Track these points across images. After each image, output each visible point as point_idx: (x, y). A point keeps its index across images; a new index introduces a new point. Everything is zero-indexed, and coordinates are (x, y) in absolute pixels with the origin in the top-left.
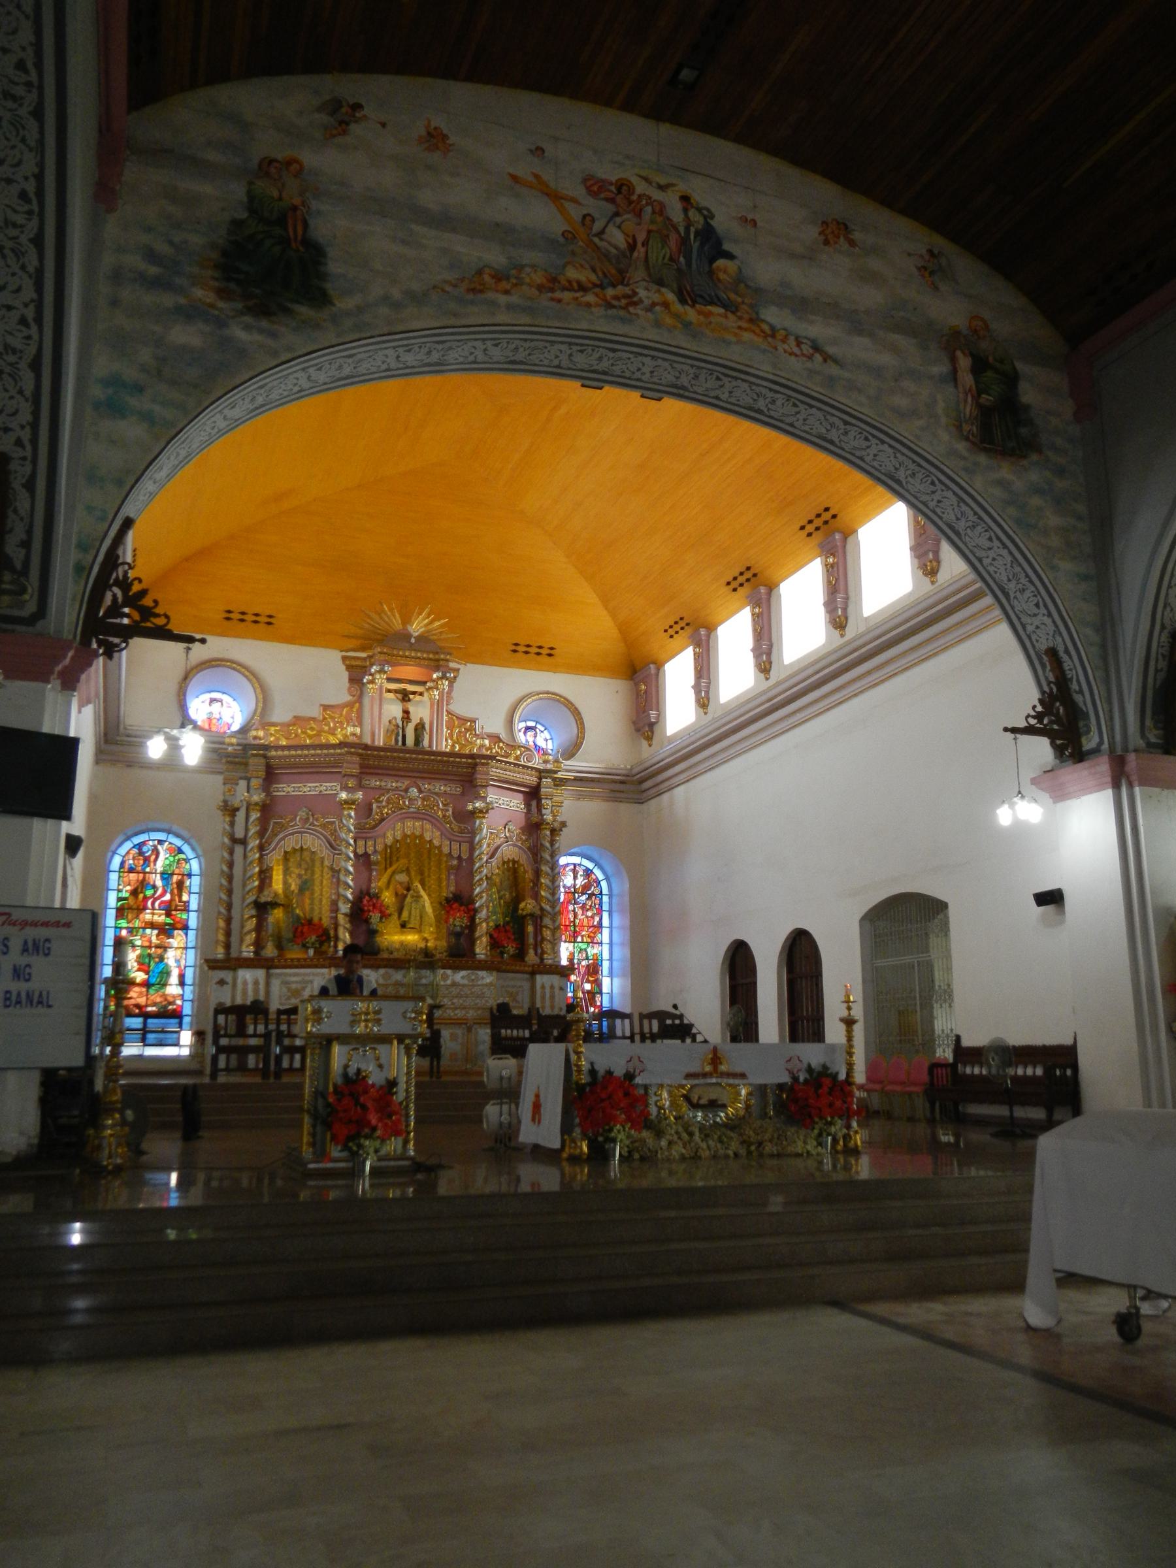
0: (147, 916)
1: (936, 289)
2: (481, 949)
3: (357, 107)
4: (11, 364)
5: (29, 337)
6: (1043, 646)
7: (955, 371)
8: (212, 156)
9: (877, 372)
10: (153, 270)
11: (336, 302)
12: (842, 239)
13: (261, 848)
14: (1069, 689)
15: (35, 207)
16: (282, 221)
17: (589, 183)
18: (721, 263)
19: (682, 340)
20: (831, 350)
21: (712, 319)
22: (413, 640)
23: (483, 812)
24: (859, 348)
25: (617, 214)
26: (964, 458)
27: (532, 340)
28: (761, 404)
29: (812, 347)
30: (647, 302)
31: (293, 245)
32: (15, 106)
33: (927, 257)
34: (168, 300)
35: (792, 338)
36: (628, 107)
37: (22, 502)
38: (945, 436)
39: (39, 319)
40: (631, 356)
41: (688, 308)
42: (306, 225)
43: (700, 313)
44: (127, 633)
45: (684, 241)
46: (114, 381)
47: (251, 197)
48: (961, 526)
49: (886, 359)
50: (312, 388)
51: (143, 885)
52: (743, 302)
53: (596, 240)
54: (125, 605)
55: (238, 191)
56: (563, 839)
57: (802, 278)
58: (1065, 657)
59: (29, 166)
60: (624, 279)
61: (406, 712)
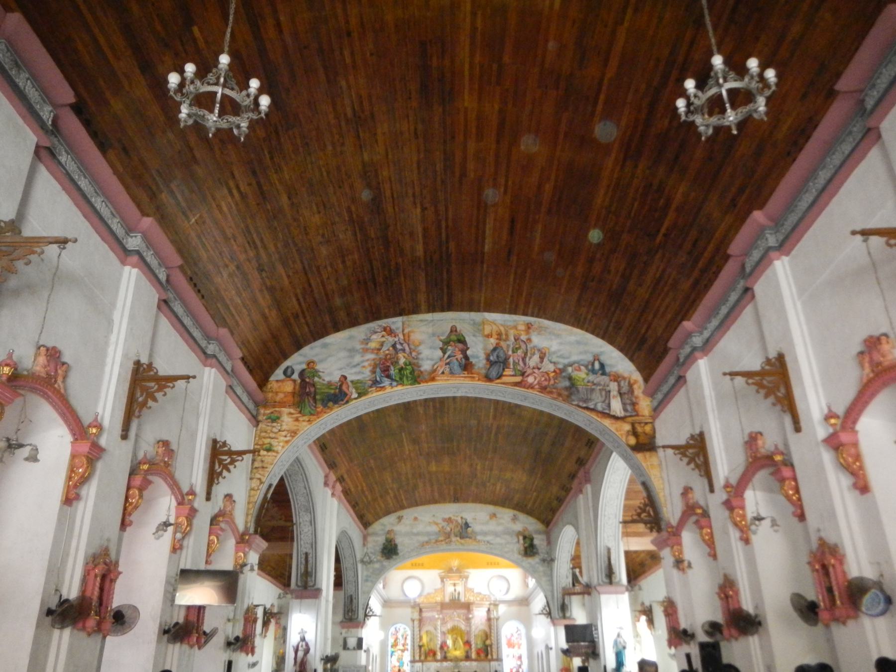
0: (398, 647)
1: (514, 523)
2: (474, 656)
3: (402, 517)
8: (381, 532)
13: (420, 631)
16: (391, 541)
18: (469, 529)
19: (461, 547)
20: (492, 542)
23: (473, 618)
24: (498, 540)
36: (450, 502)
37: (354, 601)
44: (370, 616)
45: (461, 527)
46: (367, 576)
49: (503, 541)
51: (396, 639)
55: (384, 538)
56: (500, 621)
57: (485, 528)
61: (455, 590)
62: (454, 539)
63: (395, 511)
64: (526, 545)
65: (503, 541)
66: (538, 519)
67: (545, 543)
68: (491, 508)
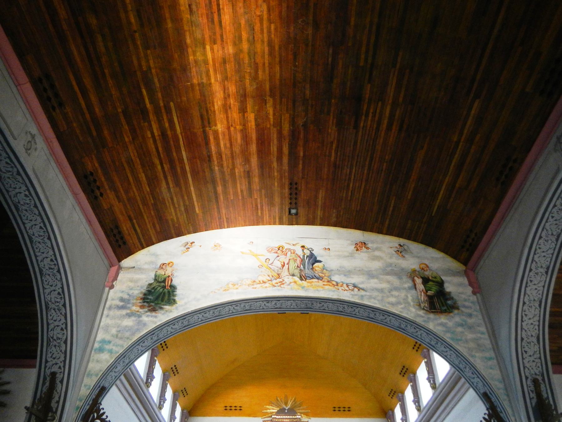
1: (403, 257)
4: (59, 343)
5: (64, 334)
6: (482, 392)
7: (415, 285)
8: (146, 266)
9: (381, 291)
10: (121, 304)
11: (178, 303)
12: (363, 247)
14: (497, 411)
15: (62, 296)
16: (164, 281)
17: (268, 249)
18: (316, 264)
20: (361, 286)
21: (313, 284)
22: (286, 411)
24: (374, 283)
25: (278, 256)
26: (423, 317)
27: (248, 302)
28: (341, 309)
29: (353, 286)
30: (288, 283)
31: (167, 288)
32: (52, 271)
33: (399, 247)
34: (124, 312)
35: (345, 285)
37: (59, 385)
38: (413, 310)
39: (66, 328)
40: (286, 301)
41: (303, 281)
42: (172, 280)
43: (308, 282)
45: (302, 261)
46: (103, 341)
47: (156, 276)
48: (433, 343)
50: (175, 331)
52: (325, 276)
53: (270, 266)
54: (97, 418)
58: (491, 396)
59: (59, 285)
60: (279, 277)
62: (288, 279)
63: (179, 234)
64: (429, 293)
65: (384, 285)
66: (446, 250)
67: (469, 290)
68: (357, 235)
